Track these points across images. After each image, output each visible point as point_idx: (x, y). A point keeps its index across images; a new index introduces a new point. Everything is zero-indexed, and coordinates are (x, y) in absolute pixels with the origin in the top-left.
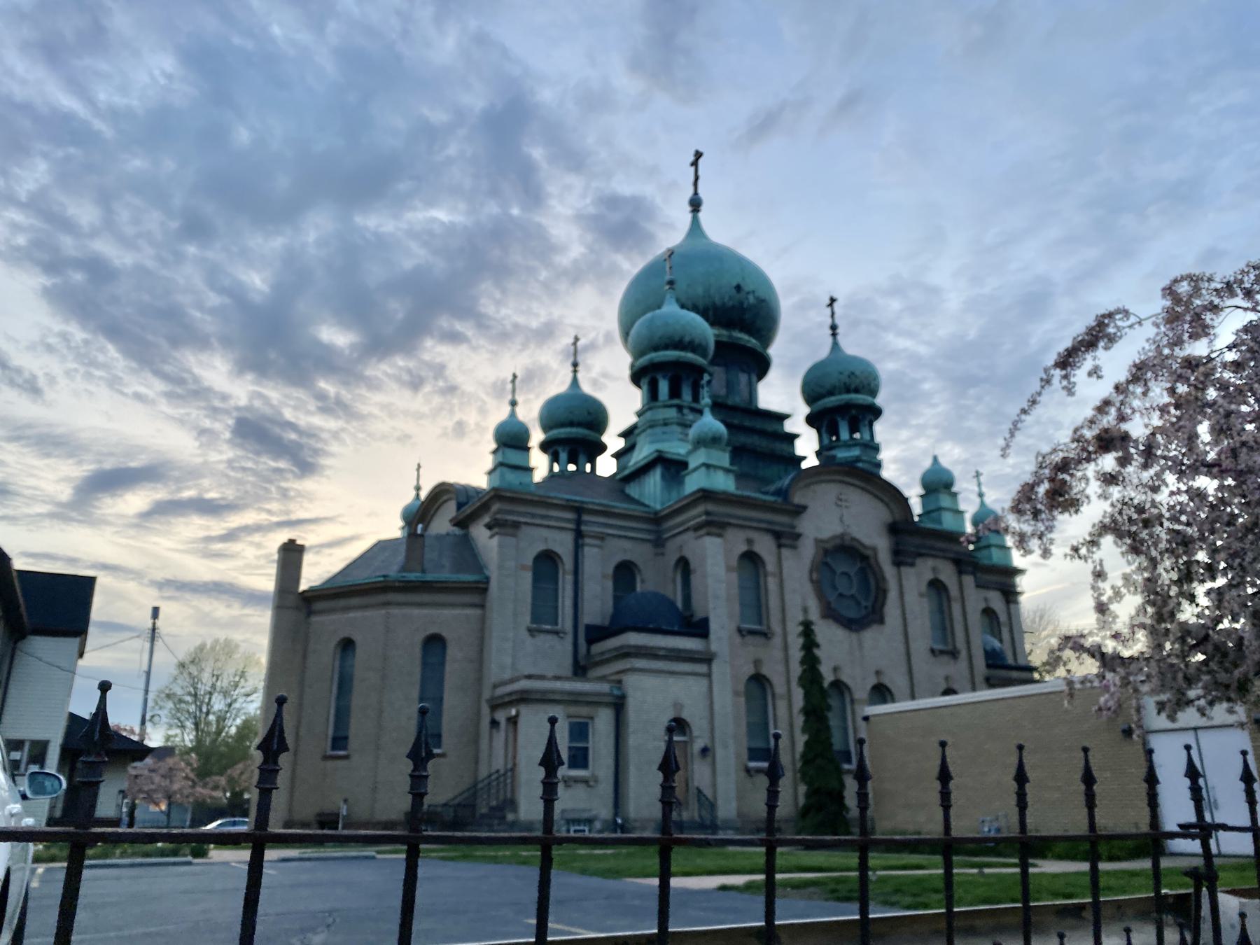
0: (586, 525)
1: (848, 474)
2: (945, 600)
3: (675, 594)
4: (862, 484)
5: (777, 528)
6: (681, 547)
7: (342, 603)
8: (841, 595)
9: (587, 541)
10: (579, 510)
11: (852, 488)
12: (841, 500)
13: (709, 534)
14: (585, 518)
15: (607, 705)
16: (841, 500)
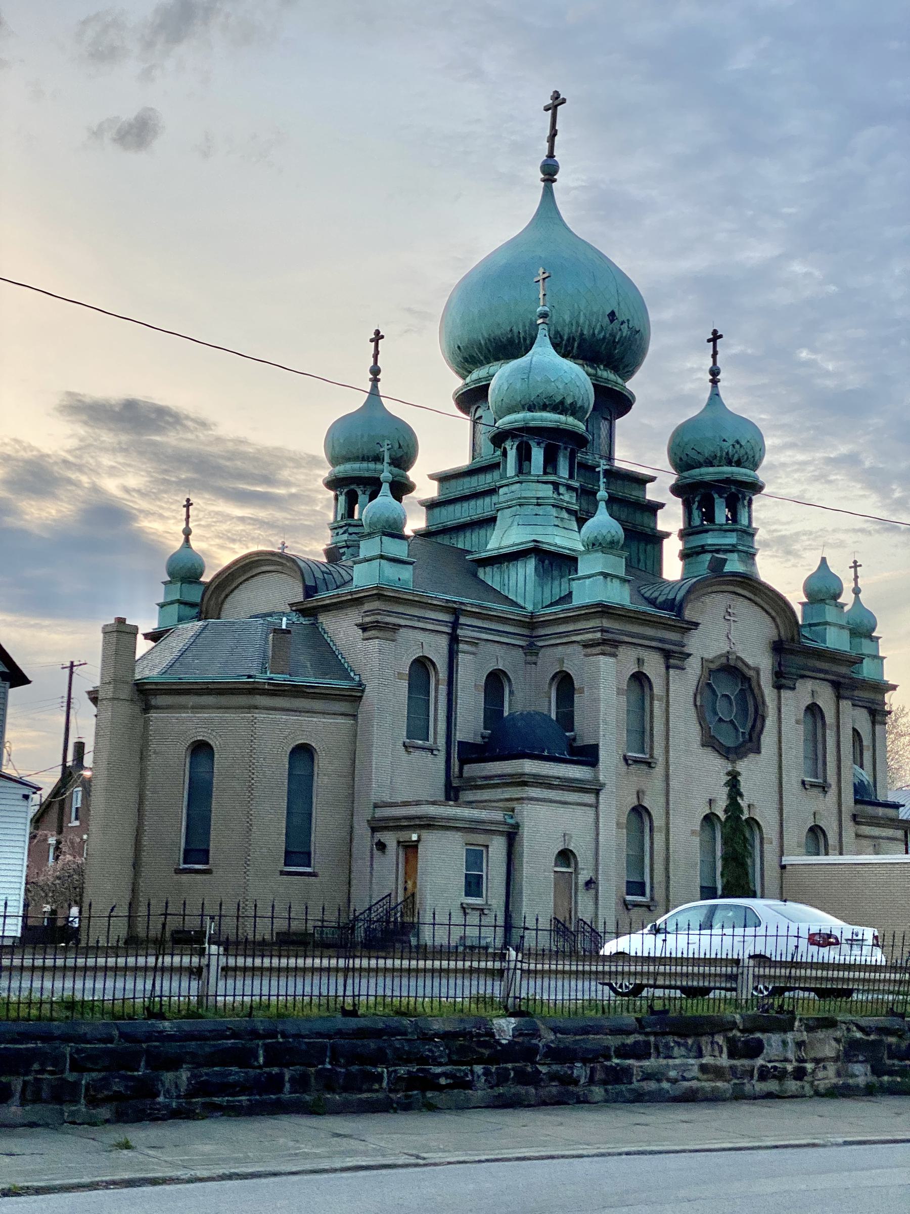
0: (462, 629)
1: (741, 584)
2: (819, 724)
3: (550, 710)
4: (752, 597)
5: (667, 647)
6: (561, 661)
7: (192, 700)
8: (721, 720)
9: (462, 646)
10: (456, 612)
11: (741, 599)
12: (729, 614)
13: (603, 654)
14: (462, 620)
15: (500, 833)
16: (729, 614)
